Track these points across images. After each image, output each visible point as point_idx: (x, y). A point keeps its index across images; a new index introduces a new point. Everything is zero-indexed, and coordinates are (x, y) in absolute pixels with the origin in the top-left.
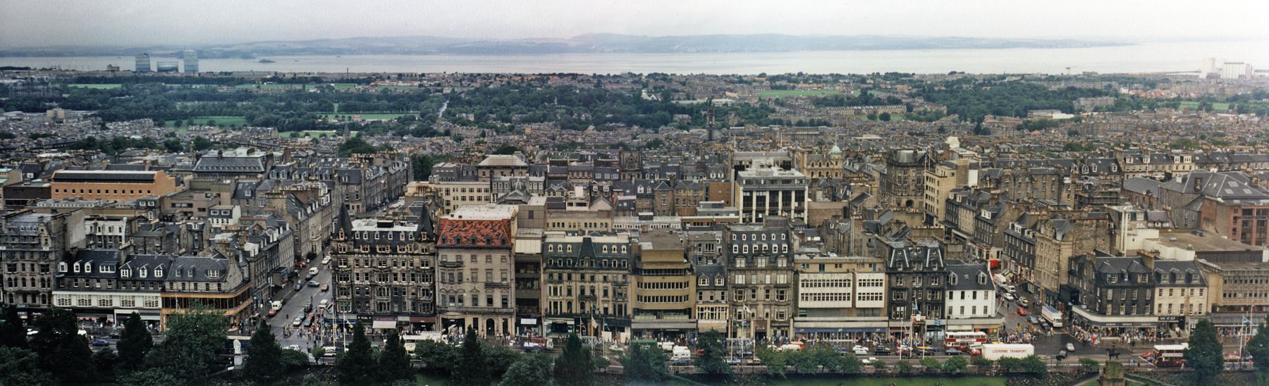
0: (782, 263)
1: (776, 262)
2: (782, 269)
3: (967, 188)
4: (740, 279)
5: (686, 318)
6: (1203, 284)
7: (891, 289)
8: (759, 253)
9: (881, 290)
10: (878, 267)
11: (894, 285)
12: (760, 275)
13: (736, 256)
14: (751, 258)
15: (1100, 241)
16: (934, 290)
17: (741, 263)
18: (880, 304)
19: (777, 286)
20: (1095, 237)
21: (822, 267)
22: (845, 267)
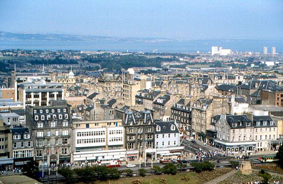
0: (65, 124)
1: (62, 124)
2: (65, 128)
3: (146, 90)
4: (40, 134)
5: (6, 158)
6: (275, 126)
7: (126, 135)
8: (51, 119)
9: (122, 135)
10: (118, 124)
11: (128, 133)
12: (52, 130)
13: (38, 121)
14: (46, 122)
15: (224, 108)
16: (149, 134)
17: (40, 125)
18: (122, 143)
19: (62, 137)
20: (223, 107)
21: (88, 126)
22: (100, 125)
